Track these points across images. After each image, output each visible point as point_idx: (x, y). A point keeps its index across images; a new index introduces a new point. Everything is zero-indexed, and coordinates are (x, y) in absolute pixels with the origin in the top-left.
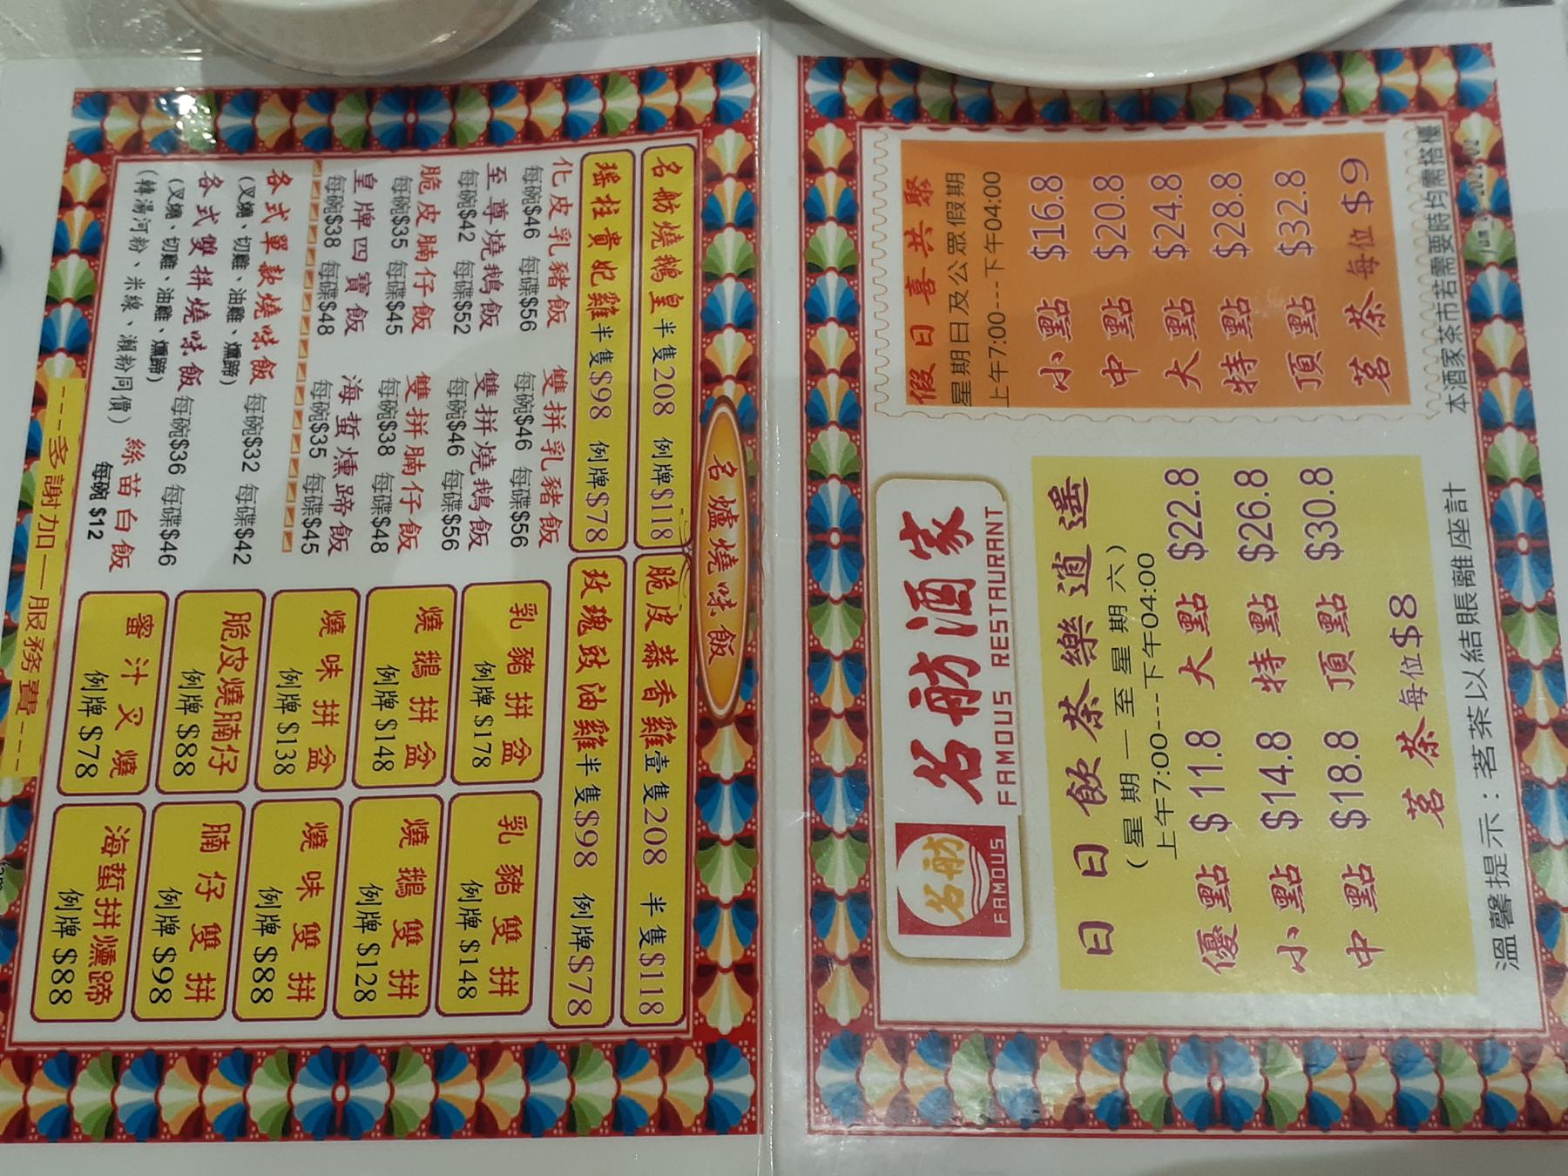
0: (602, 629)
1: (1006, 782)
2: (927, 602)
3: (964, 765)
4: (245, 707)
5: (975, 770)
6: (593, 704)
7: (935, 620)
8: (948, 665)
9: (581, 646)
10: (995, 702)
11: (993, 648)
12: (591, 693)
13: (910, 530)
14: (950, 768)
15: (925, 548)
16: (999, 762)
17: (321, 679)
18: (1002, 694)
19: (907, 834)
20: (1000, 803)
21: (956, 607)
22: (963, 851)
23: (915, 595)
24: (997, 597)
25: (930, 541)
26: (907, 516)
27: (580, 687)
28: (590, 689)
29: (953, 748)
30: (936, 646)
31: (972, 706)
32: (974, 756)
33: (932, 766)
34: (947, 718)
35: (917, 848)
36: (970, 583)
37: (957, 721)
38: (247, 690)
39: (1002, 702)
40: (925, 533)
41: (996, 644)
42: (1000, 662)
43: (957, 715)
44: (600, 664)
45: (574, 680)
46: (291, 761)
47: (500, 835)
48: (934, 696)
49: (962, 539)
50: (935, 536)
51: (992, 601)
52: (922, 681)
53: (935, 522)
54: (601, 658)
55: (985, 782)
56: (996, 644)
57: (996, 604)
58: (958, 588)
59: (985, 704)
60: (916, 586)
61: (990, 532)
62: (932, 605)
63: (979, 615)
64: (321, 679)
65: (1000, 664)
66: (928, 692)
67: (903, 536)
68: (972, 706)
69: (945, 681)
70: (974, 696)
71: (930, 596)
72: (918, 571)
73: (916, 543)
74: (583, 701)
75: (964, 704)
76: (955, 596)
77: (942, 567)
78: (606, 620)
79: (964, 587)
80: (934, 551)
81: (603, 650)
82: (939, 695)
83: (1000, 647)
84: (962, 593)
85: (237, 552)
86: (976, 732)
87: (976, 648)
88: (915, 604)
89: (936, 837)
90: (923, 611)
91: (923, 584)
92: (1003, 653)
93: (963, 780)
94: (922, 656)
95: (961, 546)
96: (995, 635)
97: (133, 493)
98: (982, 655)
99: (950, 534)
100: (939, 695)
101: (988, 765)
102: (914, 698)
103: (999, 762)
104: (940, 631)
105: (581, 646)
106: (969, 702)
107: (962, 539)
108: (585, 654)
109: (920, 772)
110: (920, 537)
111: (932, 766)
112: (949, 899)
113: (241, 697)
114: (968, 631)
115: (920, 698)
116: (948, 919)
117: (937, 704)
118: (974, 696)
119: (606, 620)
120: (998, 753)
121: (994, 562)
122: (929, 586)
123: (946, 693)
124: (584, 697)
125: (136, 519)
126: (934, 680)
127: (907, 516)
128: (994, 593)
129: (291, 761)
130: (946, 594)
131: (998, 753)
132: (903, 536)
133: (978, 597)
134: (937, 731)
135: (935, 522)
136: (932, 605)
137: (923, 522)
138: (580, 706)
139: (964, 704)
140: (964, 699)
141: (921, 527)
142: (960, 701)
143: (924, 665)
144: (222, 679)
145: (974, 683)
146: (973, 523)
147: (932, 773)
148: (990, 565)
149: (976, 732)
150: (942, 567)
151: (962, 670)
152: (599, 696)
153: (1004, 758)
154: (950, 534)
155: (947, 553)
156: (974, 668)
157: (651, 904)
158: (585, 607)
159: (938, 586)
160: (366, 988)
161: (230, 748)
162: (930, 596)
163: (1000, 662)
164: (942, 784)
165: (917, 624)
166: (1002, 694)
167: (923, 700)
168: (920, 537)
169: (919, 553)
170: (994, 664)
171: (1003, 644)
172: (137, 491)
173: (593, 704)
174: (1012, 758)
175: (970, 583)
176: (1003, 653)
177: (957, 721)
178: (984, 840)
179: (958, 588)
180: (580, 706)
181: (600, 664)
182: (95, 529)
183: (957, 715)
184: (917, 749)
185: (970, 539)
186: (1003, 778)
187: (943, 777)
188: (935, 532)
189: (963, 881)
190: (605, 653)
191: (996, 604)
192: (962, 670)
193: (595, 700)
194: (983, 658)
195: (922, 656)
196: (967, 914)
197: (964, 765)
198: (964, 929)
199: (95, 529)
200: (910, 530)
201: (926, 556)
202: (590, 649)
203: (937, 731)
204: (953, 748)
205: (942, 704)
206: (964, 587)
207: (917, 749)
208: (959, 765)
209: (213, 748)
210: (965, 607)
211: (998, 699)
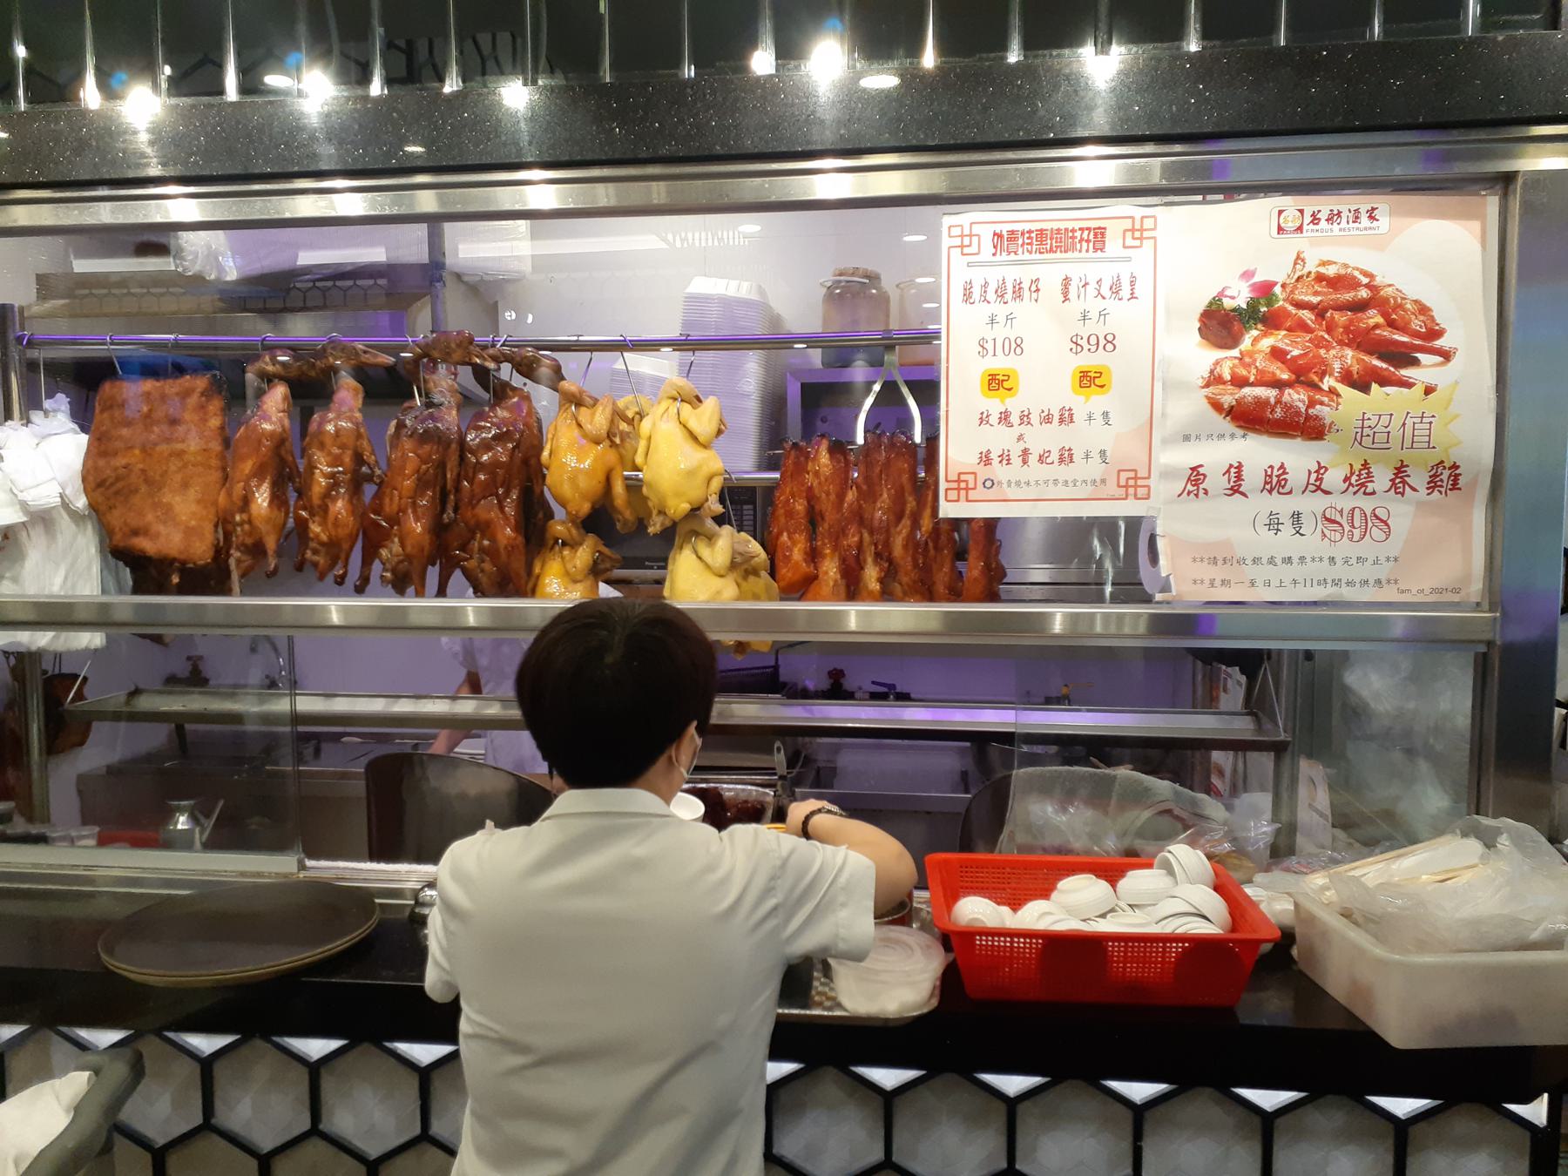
13: (1373, 209)
14: (1315, 219)
19: (1301, 211)
29: (1319, 219)
42: (1340, 230)
52: (1336, 212)
55: (1311, 226)
63: (1351, 225)
72: (1363, 210)
86: (1323, 224)
87: (1344, 224)
93: (1312, 222)
98: (1342, 226)
101: (1316, 227)
112: (1286, 221)
116: (1281, 221)
133: (1356, 225)
134: (1323, 216)
137: (1375, 212)
143: (1339, 213)
145: (1335, 224)
147: (1313, 215)
149: (1323, 224)
154: (1372, 218)
165: (1350, 211)
178: (1300, 229)
184: (1319, 211)
189: (1290, 224)
194: (1341, 226)
196: (1283, 225)
198: (1279, 225)
200: (1373, 209)
203: (1323, 216)
204: (1319, 219)
207: (1319, 211)
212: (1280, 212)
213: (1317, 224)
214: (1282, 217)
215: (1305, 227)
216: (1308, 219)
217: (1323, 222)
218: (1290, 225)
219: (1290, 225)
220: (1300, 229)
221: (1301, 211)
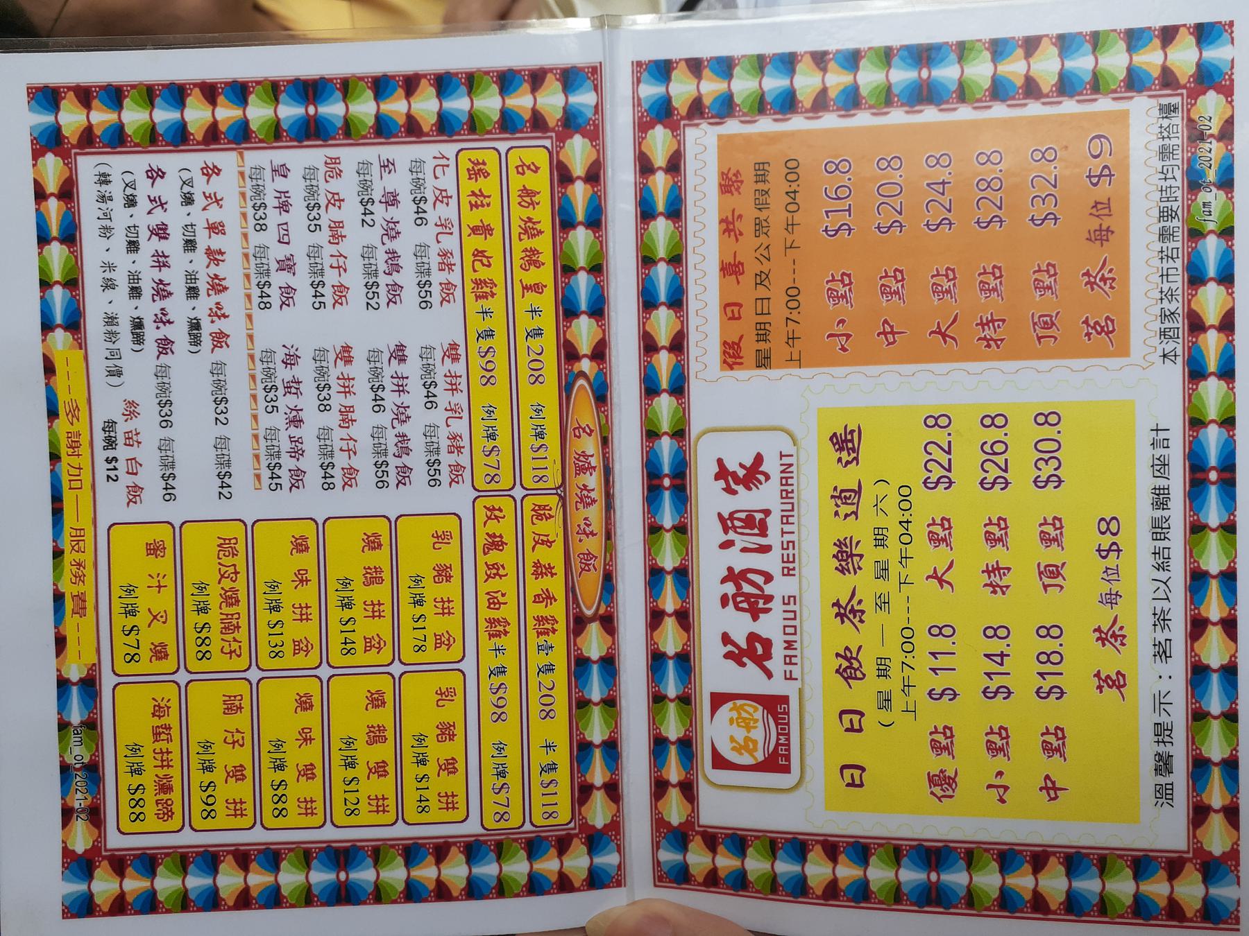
0: (501, 550)
1: (791, 663)
2: (734, 528)
3: (760, 651)
4: (242, 608)
5: (768, 655)
6: (497, 606)
7: (741, 542)
8: (750, 576)
9: (486, 563)
10: (784, 604)
11: (783, 562)
12: (496, 598)
13: (723, 473)
14: (750, 653)
15: (734, 486)
16: (785, 648)
17: (296, 588)
18: (789, 597)
19: (718, 700)
20: (786, 679)
21: (756, 531)
22: (758, 712)
23: (726, 522)
24: (788, 523)
25: (738, 481)
26: (720, 462)
27: (488, 594)
28: (495, 595)
29: (753, 638)
30: (741, 562)
31: (767, 606)
32: (767, 644)
33: (737, 652)
34: (748, 616)
35: (725, 711)
36: (767, 512)
37: (755, 618)
38: (242, 596)
39: (789, 604)
40: (734, 474)
41: (785, 559)
42: (788, 572)
43: (755, 614)
44: (501, 576)
45: (484, 588)
46: (281, 649)
47: (437, 701)
48: (739, 599)
49: (762, 478)
50: (741, 477)
51: (784, 526)
52: (730, 588)
53: (741, 466)
54: (501, 572)
55: (776, 664)
56: (785, 559)
57: (787, 528)
58: (758, 516)
59: (776, 605)
60: (726, 515)
61: (782, 472)
62: (739, 530)
63: (773, 537)
64: (296, 588)
65: (788, 575)
66: (734, 596)
67: (717, 477)
68: (767, 606)
69: (747, 588)
70: (769, 599)
71: (737, 523)
72: (728, 504)
73: (727, 482)
74: (490, 604)
75: (761, 605)
76: (755, 523)
77: (747, 500)
78: (504, 544)
79: (761, 516)
80: (740, 489)
81: (503, 566)
82: (743, 599)
83: (788, 562)
84: (761, 520)
85: (220, 490)
86: (770, 626)
88: (726, 531)
89: (739, 702)
90: (732, 535)
91: (731, 514)
92: (791, 565)
94: (730, 569)
95: (761, 483)
96: (785, 552)
97: (136, 444)
99: (753, 475)
100: (743, 599)
101: (778, 651)
102: (724, 601)
103: (785, 648)
104: (744, 550)
105: (486, 563)
106: (764, 604)
107: (762, 478)
108: (489, 569)
109: (728, 656)
110: (730, 478)
111: (737, 652)
113: (238, 601)
114: (765, 549)
115: (729, 600)
117: (740, 605)
118: (769, 599)
119: (504, 544)
120: (785, 642)
121: (786, 495)
122: (736, 515)
123: (748, 597)
124: (491, 601)
125: (141, 465)
126: (739, 587)
127: (720, 462)
128: (786, 519)
129: (281, 649)
130: (749, 522)
131: (785, 642)
132: (717, 477)
133: (773, 523)
134: (740, 625)
135: (741, 466)
136: (739, 530)
137: (732, 466)
138: (489, 607)
139: (761, 605)
140: (761, 602)
141: (731, 470)
142: (757, 603)
143: (732, 576)
144: (222, 588)
145: (768, 589)
146: (771, 466)
147: (736, 657)
148: (782, 498)
149: (770, 626)
150: (747, 500)
151: (759, 579)
152: (502, 600)
153: (789, 645)
154: (753, 475)
155: (749, 489)
156: (769, 578)
157: (547, 747)
158: (487, 534)
159: (743, 515)
160: (353, 807)
161: (235, 640)
162: (737, 523)
163: (788, 572)
164: (743, 665)
165: (727, 545)
166: (789, 597)
167: (731, 602)
168: (730, 478)
169: (730, 491)
170: (784, 575)
171: (791, 559)
172: (139, 443)
173: (497, 606)
174: (796, 645)
175: (767, 512)
176: (791, 565)
177: (755, 618)
179: (758, 516)
180: (489, 607)
181: (501, 576)
182: (112, 474)
183: (755, 614)
184: (726, 639)
185: (767, 477)
186: (789, 660)
187: (745, 660)
188: (741, 473)
190: (504, 568)
191: (787, 528)
192: (759, 579)
193: (500, 603)
195: (730, 569)
197: (760, 651)
199: (112, 474)
200: (723, 473)
201: (734, 492)
202: (493, 565)
203: (740, 625)
204: (753, 638)
205: (745, 605)
206: (761, 516)
207: (726, 639)
208: (756, 650)
209: (222, 639)
210: (763, 532)
211: (786, 601)
213: (767, 644)
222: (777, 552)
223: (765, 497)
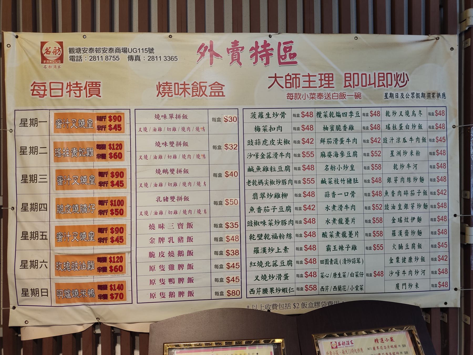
5: (339, 345)
7: (347, 343)
14: (339, 344)
19: (336, 342)
32: (340, 345)
52: (344, 342)
59: (343, 346)
63: (348, 345)
72: (349, 341)
77: (350, 343)
93: (339, 345)
112: (333, 345)
116: (332, 345)
121: (351, 346)
128: (349, 346)
130: (349, 343)
143: (344, 342)
149: (342, 346)
150: (350, 343)
156: (345, 345)
189: (334, 346)
200: (352, 341)
212: (331, 343)
213: (340, 345)
214: (332, 344)
215: (338, 347)
216: (338, 344)
217: (341, 345)
218: (334, 346)
219: (334, 346)
220: (337, 347)
221: (336, 342)
222: (347, 346)
223: (351, 344)
